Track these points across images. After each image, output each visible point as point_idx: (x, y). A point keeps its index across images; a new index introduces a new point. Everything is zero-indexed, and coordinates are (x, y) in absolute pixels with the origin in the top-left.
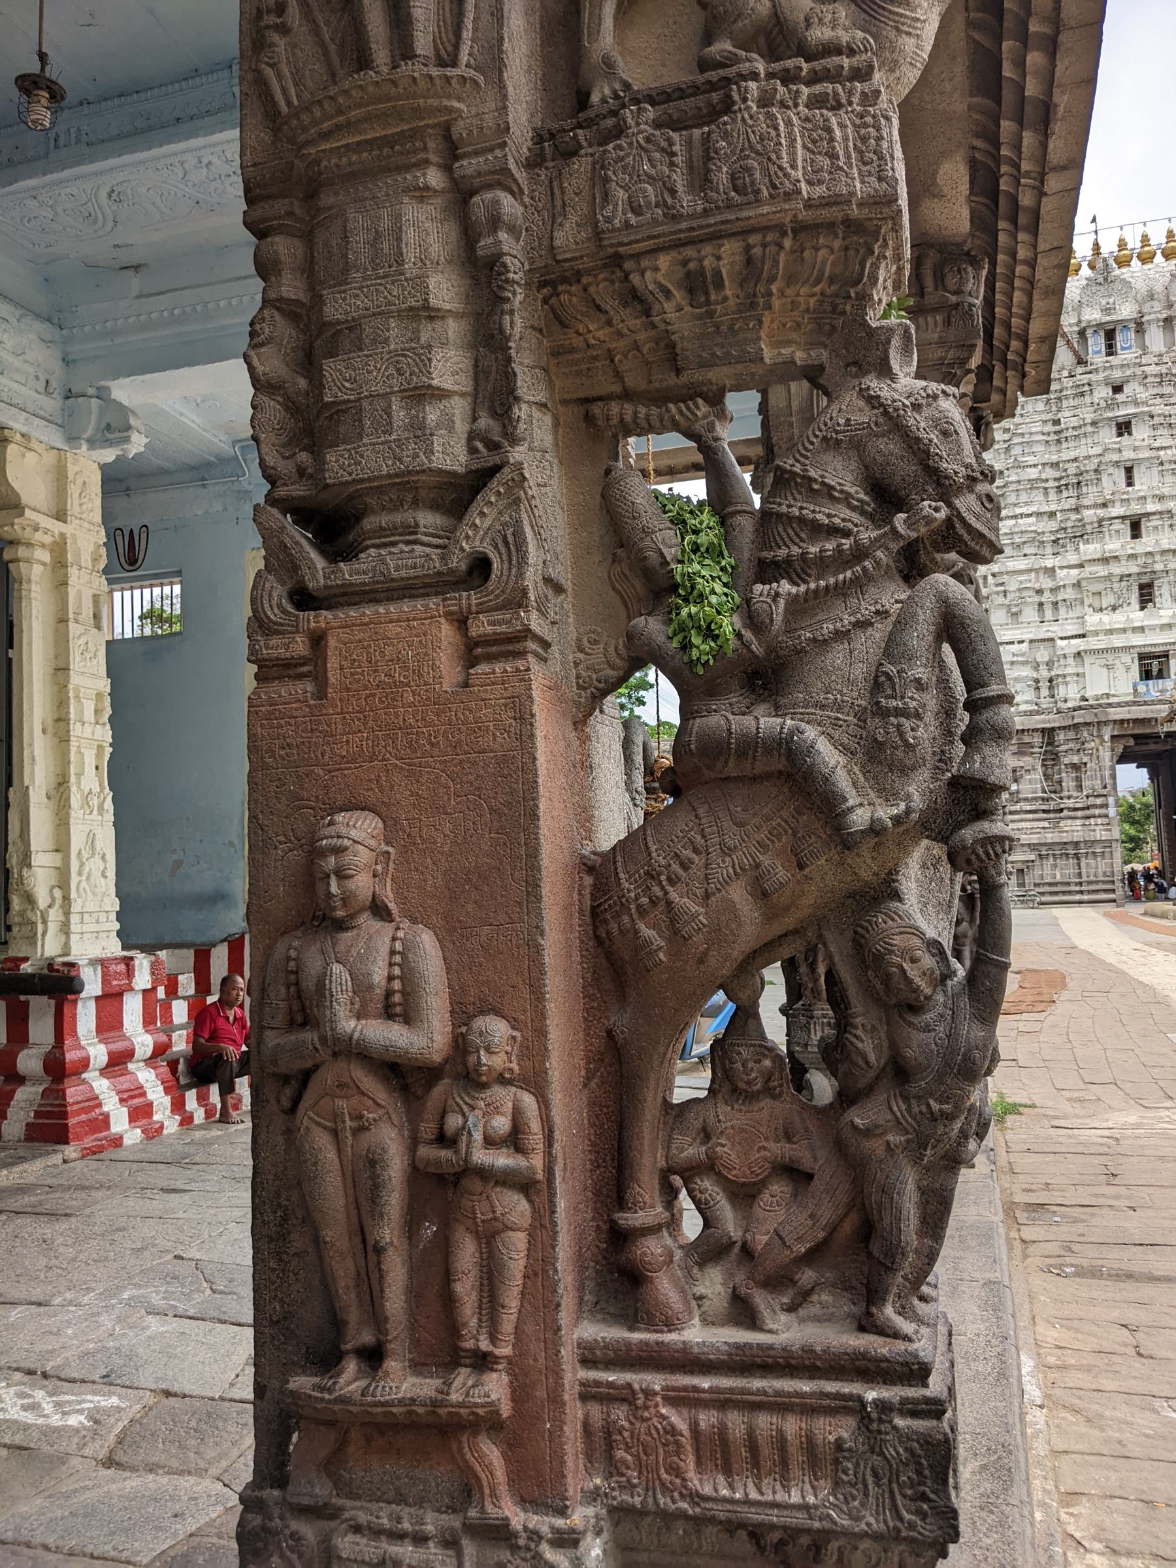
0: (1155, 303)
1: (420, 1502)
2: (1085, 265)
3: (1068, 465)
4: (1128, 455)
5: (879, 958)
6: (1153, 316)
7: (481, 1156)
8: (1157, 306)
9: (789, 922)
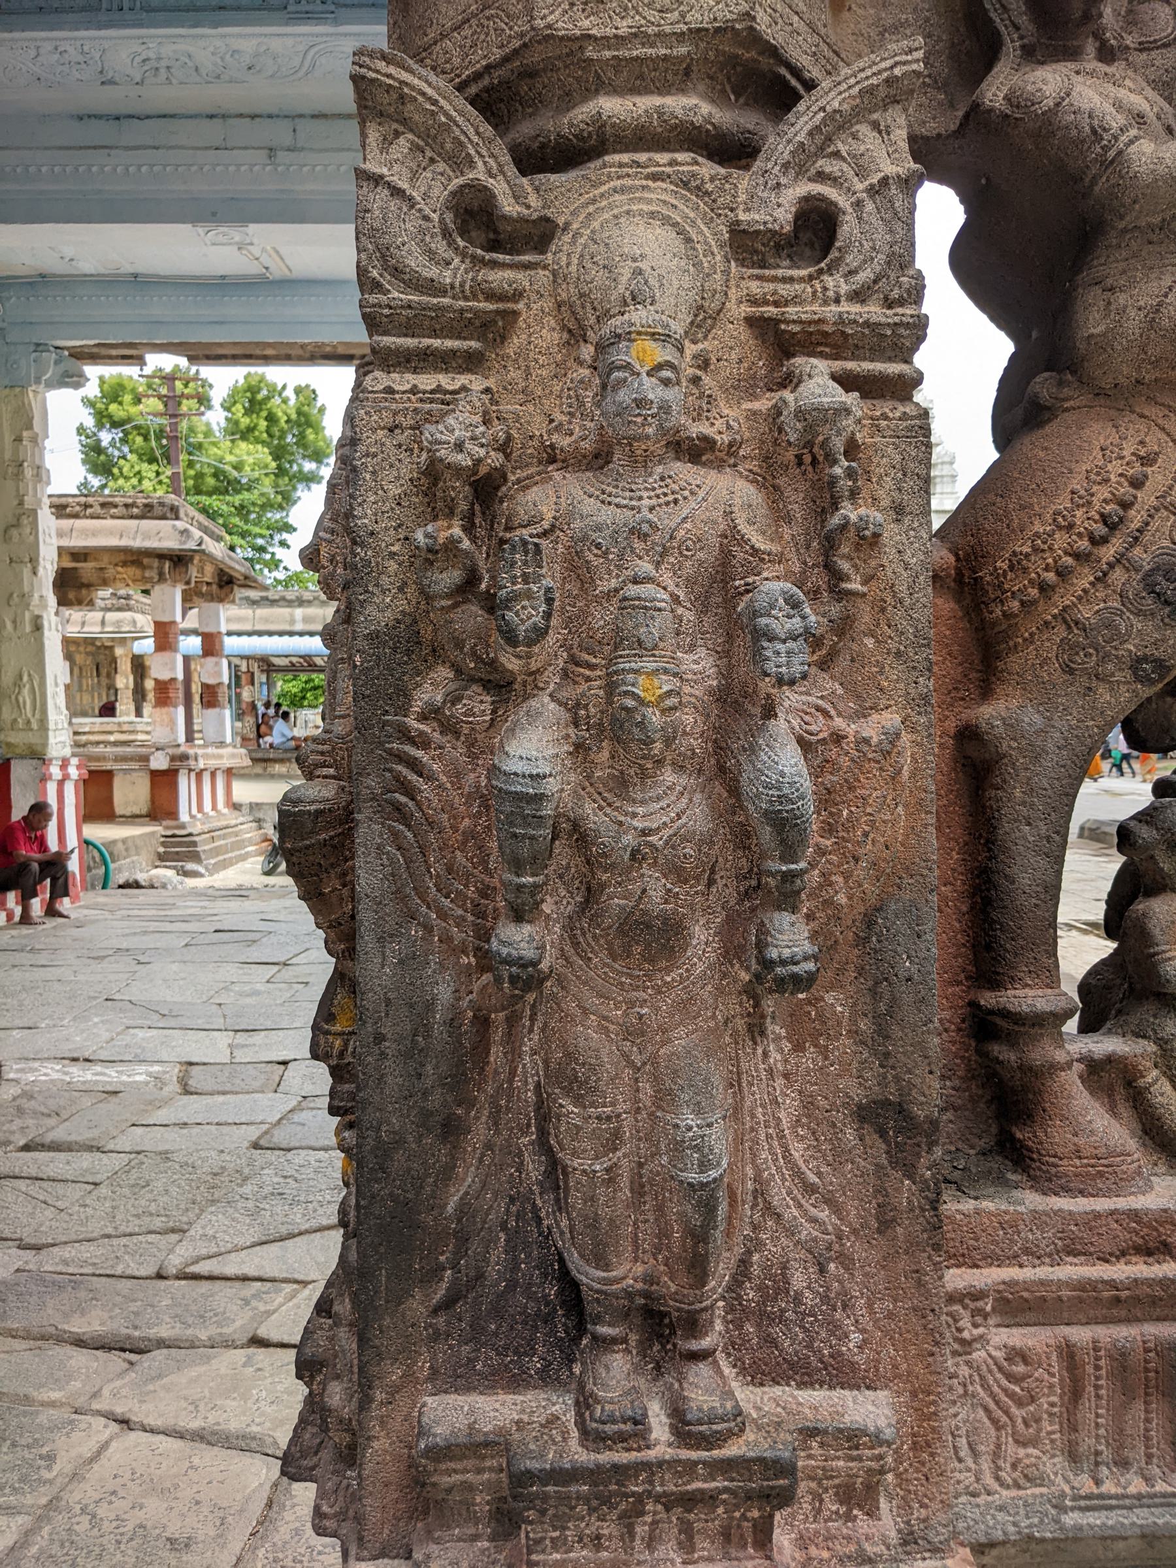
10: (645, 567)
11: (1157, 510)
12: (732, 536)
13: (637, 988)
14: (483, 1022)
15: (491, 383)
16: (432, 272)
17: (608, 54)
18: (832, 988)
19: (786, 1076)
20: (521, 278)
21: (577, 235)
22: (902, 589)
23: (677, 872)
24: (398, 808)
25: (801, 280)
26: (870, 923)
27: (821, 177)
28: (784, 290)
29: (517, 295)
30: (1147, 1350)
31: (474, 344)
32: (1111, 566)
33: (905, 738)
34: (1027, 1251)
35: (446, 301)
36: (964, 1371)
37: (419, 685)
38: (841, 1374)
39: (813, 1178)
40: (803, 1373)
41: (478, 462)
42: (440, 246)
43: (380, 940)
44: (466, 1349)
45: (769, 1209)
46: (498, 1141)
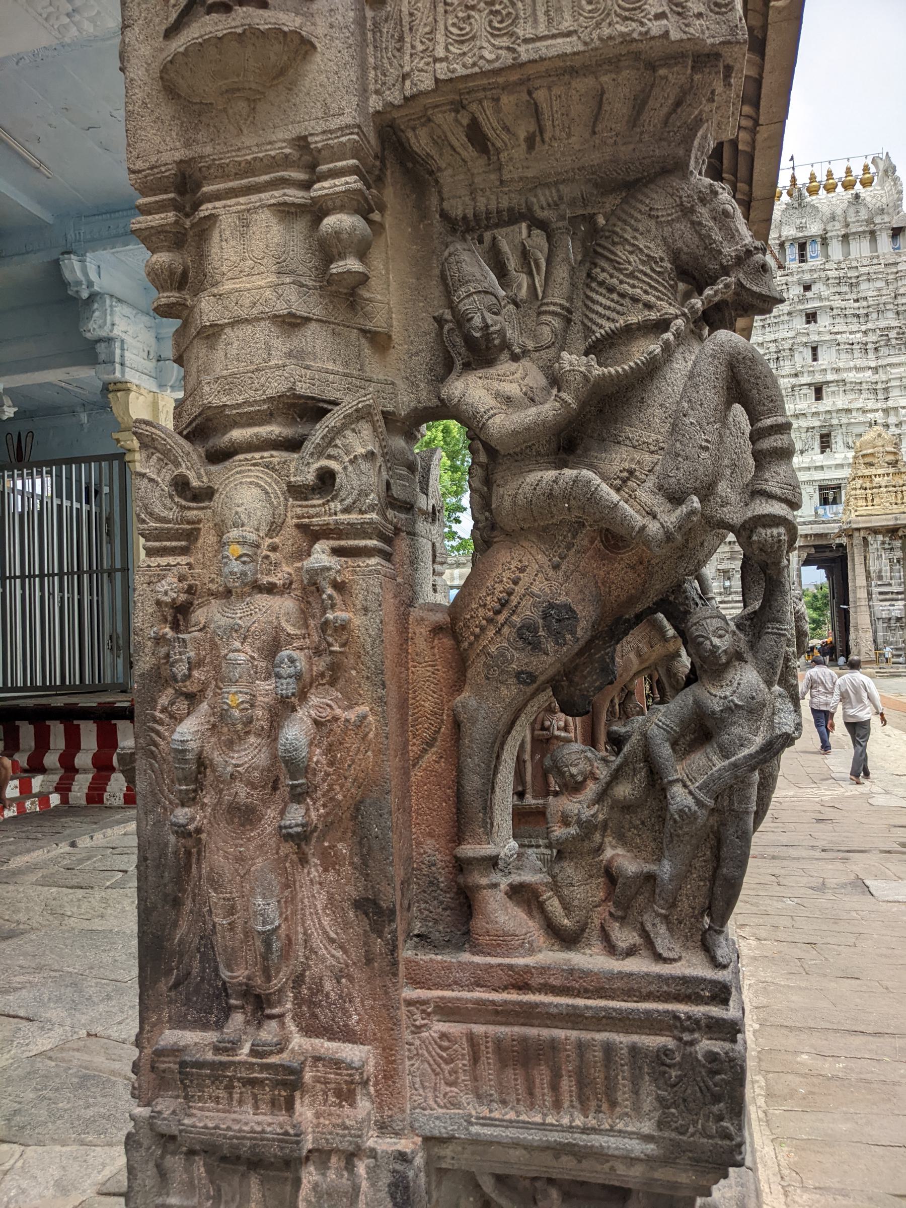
0: (836, 223)
2: (785, 192)
3: (770, 345)
4: (814, 337)
6: (834, 233)
8: (838, 225)
12: (278, 628)
13: (237, 838)
14: (188, 853)
15: (192, 560)
16: (165, 513)
17: (234, 412)
18: (340, 840)
19: (320, 884)
20: (200, 514)
22: (368, 647)
23: (251, 784)
24: (152, 752)
25: (319, 506)
26: (357, 810)
27: (330, 457)
28: (312, 511)
30: (513, 1040)
31: (183, 543)
32: (502, 625)
33: (371, 718)
34: (456, 983)
36: (417, 1042)
38: (349, 1036)
39: (333, 935)
41: (174, 600)
42: (168, 502)
43: (146, 813)
44: (183, 1009)
46: (196, 909)
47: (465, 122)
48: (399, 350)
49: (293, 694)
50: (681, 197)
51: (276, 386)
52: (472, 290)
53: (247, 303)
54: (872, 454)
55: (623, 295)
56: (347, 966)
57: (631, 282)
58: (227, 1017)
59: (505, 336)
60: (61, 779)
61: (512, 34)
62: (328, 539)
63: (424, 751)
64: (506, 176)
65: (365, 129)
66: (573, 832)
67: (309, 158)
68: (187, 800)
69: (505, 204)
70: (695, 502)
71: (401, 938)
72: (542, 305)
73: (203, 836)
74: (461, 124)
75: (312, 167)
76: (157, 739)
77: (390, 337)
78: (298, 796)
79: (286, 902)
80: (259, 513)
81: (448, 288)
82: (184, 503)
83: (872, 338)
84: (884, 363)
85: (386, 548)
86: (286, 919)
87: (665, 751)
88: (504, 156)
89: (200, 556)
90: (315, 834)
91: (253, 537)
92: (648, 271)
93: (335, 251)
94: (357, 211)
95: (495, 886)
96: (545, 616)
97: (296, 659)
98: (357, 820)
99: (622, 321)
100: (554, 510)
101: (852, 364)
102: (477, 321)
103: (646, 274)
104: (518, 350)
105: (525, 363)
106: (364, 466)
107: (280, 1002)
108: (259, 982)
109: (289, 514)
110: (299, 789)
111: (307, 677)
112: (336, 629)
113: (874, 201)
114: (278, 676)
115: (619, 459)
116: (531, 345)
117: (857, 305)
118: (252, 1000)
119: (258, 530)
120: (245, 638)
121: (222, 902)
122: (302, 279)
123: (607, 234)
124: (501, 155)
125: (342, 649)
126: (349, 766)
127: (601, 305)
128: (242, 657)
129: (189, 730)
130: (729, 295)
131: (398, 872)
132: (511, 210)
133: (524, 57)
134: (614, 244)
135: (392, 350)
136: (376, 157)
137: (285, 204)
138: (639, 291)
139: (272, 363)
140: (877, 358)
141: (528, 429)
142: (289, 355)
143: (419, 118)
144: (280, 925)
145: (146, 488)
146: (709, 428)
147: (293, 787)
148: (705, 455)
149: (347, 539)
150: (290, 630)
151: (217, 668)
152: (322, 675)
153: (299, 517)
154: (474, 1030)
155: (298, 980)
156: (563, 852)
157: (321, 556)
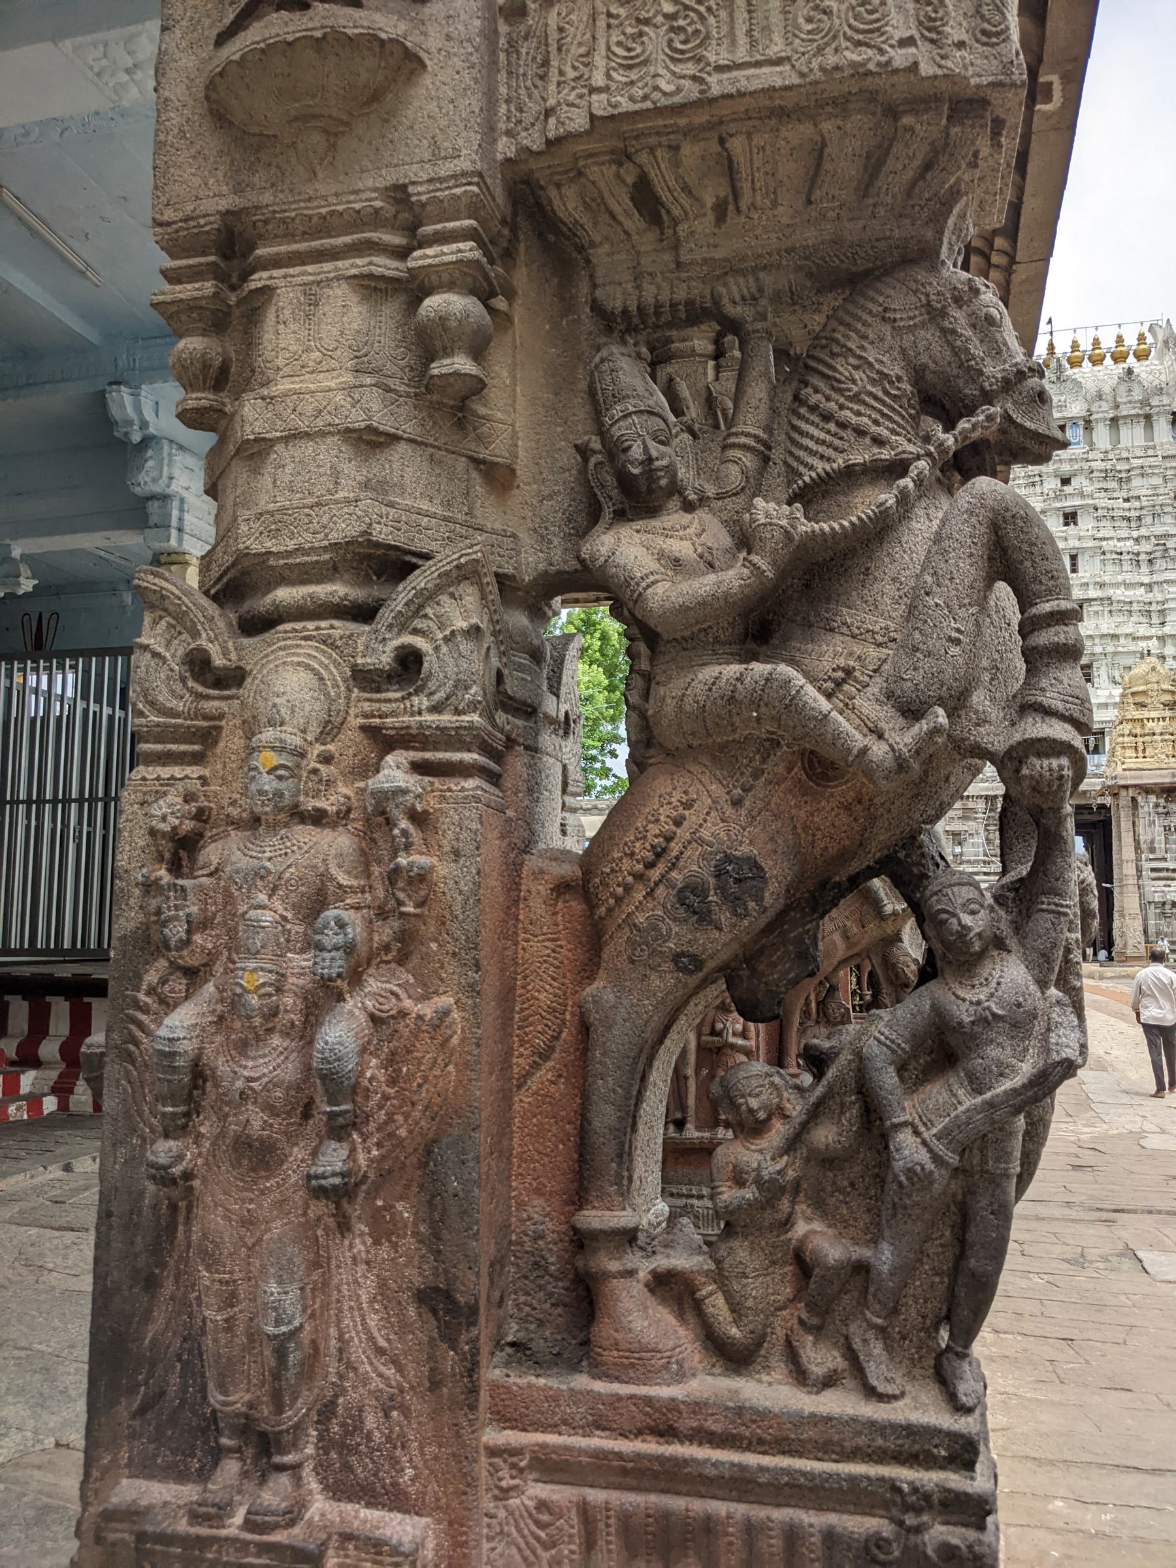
0: (1103, 403)
1: (699, 1184)
5: (894, 966)
6: (1100, 415)
7: (732, 1040)
8: (1105, 406)
9: (856, 950)
10: (262, 897)
11: (689, 842)
12: (325, 876)
13: (247, 1190)
14: (173, 1208)
15: (207, 772)
16: (173, 703)
17: (282, 562)
18: (401, 1198)
19: (368, 1263)
20: (223, 705)
21: (255, 678)
25: (397, 700)
26: (429, 1152)
27: (416, 632)
28: (385, 708)
29: (221, 717)
31: (196, 747)
32: (656, 884)
33: (455, 1015)
34: (565, 1422)
35: (179, 721)
36: (502, 1514)
37: (147, 971)
38: (398, 1501)
39: (382, 1343)
40: (368, 1495)
41: (174, 828)
42: (178, 687)
43: (114, 1145)
44: (152, 1446)
45: (350, 1366)
46: (179, 1295)
47: (630, 179)
48: (526, 489)
49: (339, 975)
50: (927, 295)
51: (344, 528)
52: (631, 409)
53: (309, 410)
54: (1144, 693)
55: (843, 425)
56: (402, 1391)
57: (856, 407)
58: (216, 1464)
59: (676, 475)
60: (60, 1076)
61: (699, 60)
62: (407, 748)
63: (536, 1066)
64: (685, 257)
65: (489, 181)
66: (749, 1196)
67: (408, 215)
68: (176, 1128)
69: (681, 294)
70: (941, 716)
71: (485, 1348)
72: (729, 435)
73: (196, 1183)
74: (623, 181)
75: (411, 229)
76: (139, 1034)
77: (513, 471)
78: (338, 1130)
79: (313, 1290)
80: (308, 708)
81: (598, 404)
82: (200, 689)
83: (1146, 547)
84: (1160, 579)
85: (492, 765)
86: (312, 1316)
87: (888, 1079)
88: (682, 230)
89: (219, 766)
90: (364, 1187)
91: (297, 741)
92: (880, 394)
93: (438, 344)
94: (473, 292)
95: (631, 1273)
96: (719, 874)
97: (348, 921)
98: (427, 1168)
99: (840, 461)
100: (736, 719)
101: (1120, 578)
102: (637, 452)
103: (876, 398)
104: (692, 497)
105: (702, 514)
106: (465, 646)
107: (295, 1445)
108: (266, 1412)
109: (352, 711)
110: (341, 1119)
111: (363, 950)
112: (410, 881)
113: (1151, 378)
114: (320, 947)
115: (832, 653)
116: (711, 490)
117: (1127, 505)
118: (254, 1438)
119: (304, 731)
120: (274, 889)
121: (217, 1286)
122: (391, 382)
123: (824, 342)
124: (679, 228)
125: (418, 911)
126: (420, 1086)
127: (812, 437)
128: (267, 917)
129: (181, 1024)
130: (991, 433)
131: (485, 1249)
132: (690, 303)
133: (716, 90)
134: (833, 355)
135: (516, 491)
136: (504, 222)
137: (371, 276)
138: (865, 420)
139: (340, 495)
140: (1152, 573)
141: (703, 604)
142: (366, 485)
143: (566, 172)
144: (302, 1325)
145: (147, 667)
146: (962, 613)
147: (332, 1116)
148: (954, 650)
149: (436, 749)
150: (343, 879)
151: (232, 932)
152: (387, 948)
153: (366, 716)
154: (590, 1498)
155: (327, 1411)
156: (732, 1225)
157: (395, 772)
